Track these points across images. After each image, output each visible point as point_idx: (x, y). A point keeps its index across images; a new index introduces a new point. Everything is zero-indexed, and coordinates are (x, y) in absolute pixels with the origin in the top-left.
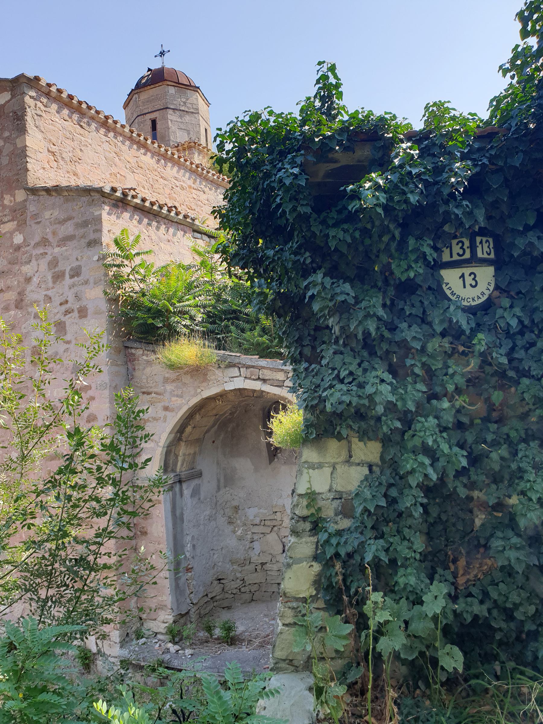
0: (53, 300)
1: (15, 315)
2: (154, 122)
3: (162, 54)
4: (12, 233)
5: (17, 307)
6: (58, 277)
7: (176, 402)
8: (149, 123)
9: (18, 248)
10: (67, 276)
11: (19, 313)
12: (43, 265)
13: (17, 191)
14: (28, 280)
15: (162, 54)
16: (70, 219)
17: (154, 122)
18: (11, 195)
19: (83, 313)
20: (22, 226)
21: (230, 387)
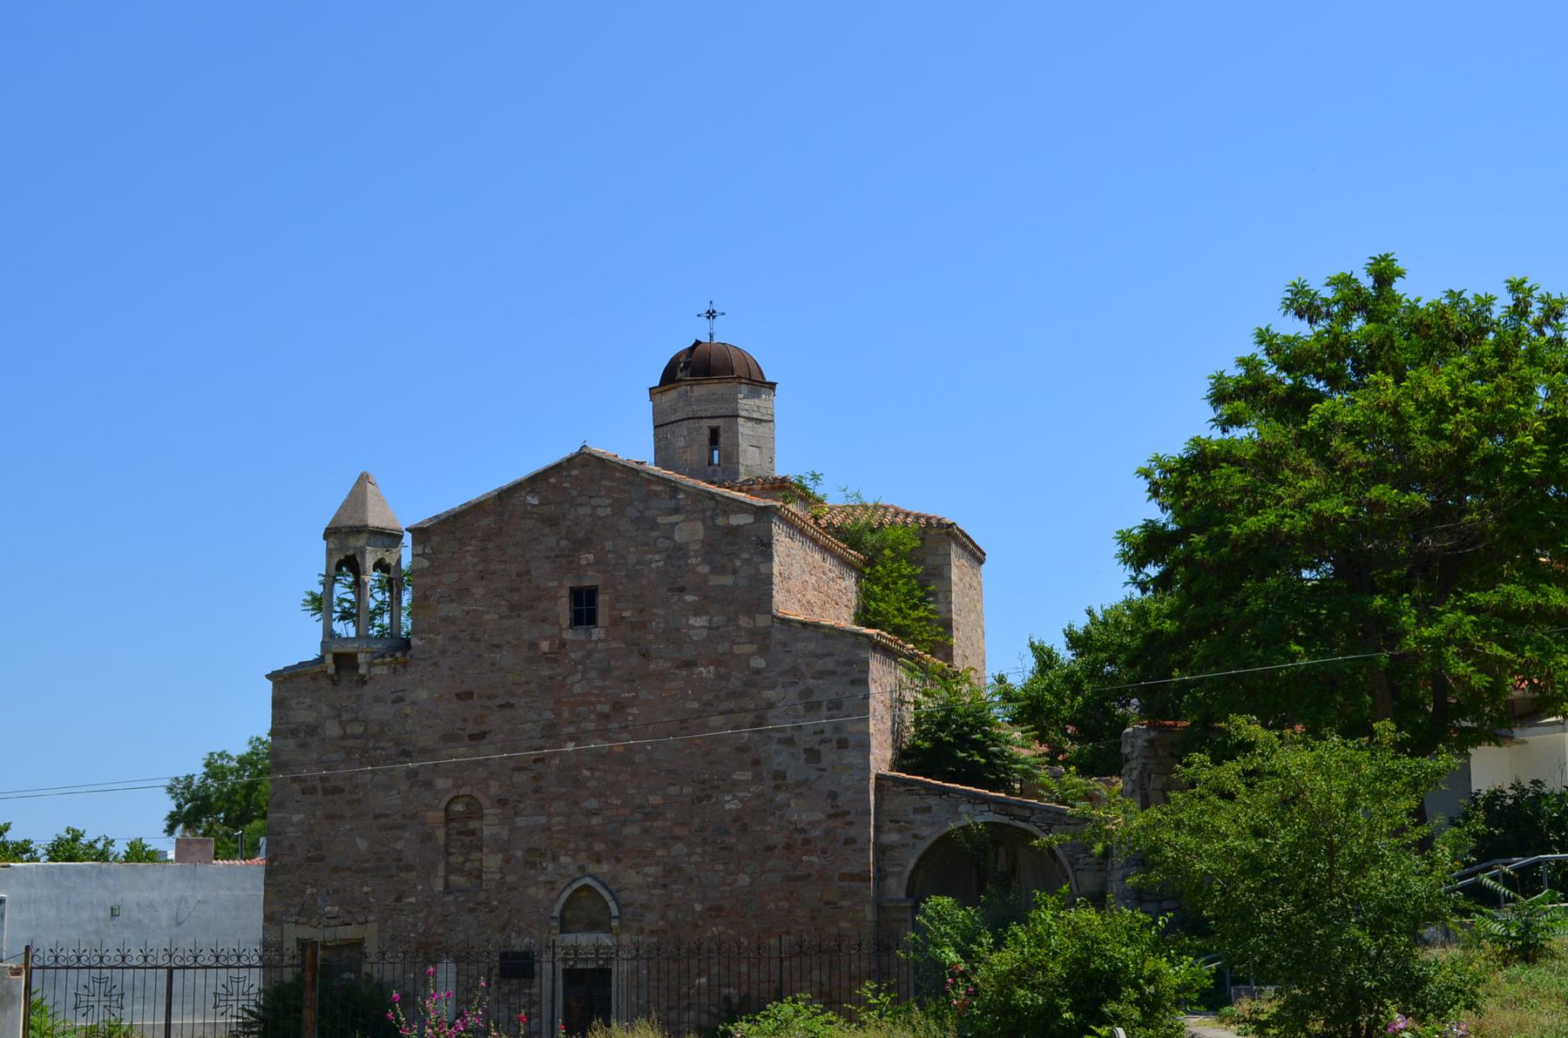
2: (714, 435)
3: (711, 314)
6: (813, 707)
8: (707, 432)
9: (758, 672)
10: (824, 708)
12: (793, 694)
15: (711, 314)
16: (829, 655)
17: (714, 435)
19: (843, 744)
20: (763, 651)
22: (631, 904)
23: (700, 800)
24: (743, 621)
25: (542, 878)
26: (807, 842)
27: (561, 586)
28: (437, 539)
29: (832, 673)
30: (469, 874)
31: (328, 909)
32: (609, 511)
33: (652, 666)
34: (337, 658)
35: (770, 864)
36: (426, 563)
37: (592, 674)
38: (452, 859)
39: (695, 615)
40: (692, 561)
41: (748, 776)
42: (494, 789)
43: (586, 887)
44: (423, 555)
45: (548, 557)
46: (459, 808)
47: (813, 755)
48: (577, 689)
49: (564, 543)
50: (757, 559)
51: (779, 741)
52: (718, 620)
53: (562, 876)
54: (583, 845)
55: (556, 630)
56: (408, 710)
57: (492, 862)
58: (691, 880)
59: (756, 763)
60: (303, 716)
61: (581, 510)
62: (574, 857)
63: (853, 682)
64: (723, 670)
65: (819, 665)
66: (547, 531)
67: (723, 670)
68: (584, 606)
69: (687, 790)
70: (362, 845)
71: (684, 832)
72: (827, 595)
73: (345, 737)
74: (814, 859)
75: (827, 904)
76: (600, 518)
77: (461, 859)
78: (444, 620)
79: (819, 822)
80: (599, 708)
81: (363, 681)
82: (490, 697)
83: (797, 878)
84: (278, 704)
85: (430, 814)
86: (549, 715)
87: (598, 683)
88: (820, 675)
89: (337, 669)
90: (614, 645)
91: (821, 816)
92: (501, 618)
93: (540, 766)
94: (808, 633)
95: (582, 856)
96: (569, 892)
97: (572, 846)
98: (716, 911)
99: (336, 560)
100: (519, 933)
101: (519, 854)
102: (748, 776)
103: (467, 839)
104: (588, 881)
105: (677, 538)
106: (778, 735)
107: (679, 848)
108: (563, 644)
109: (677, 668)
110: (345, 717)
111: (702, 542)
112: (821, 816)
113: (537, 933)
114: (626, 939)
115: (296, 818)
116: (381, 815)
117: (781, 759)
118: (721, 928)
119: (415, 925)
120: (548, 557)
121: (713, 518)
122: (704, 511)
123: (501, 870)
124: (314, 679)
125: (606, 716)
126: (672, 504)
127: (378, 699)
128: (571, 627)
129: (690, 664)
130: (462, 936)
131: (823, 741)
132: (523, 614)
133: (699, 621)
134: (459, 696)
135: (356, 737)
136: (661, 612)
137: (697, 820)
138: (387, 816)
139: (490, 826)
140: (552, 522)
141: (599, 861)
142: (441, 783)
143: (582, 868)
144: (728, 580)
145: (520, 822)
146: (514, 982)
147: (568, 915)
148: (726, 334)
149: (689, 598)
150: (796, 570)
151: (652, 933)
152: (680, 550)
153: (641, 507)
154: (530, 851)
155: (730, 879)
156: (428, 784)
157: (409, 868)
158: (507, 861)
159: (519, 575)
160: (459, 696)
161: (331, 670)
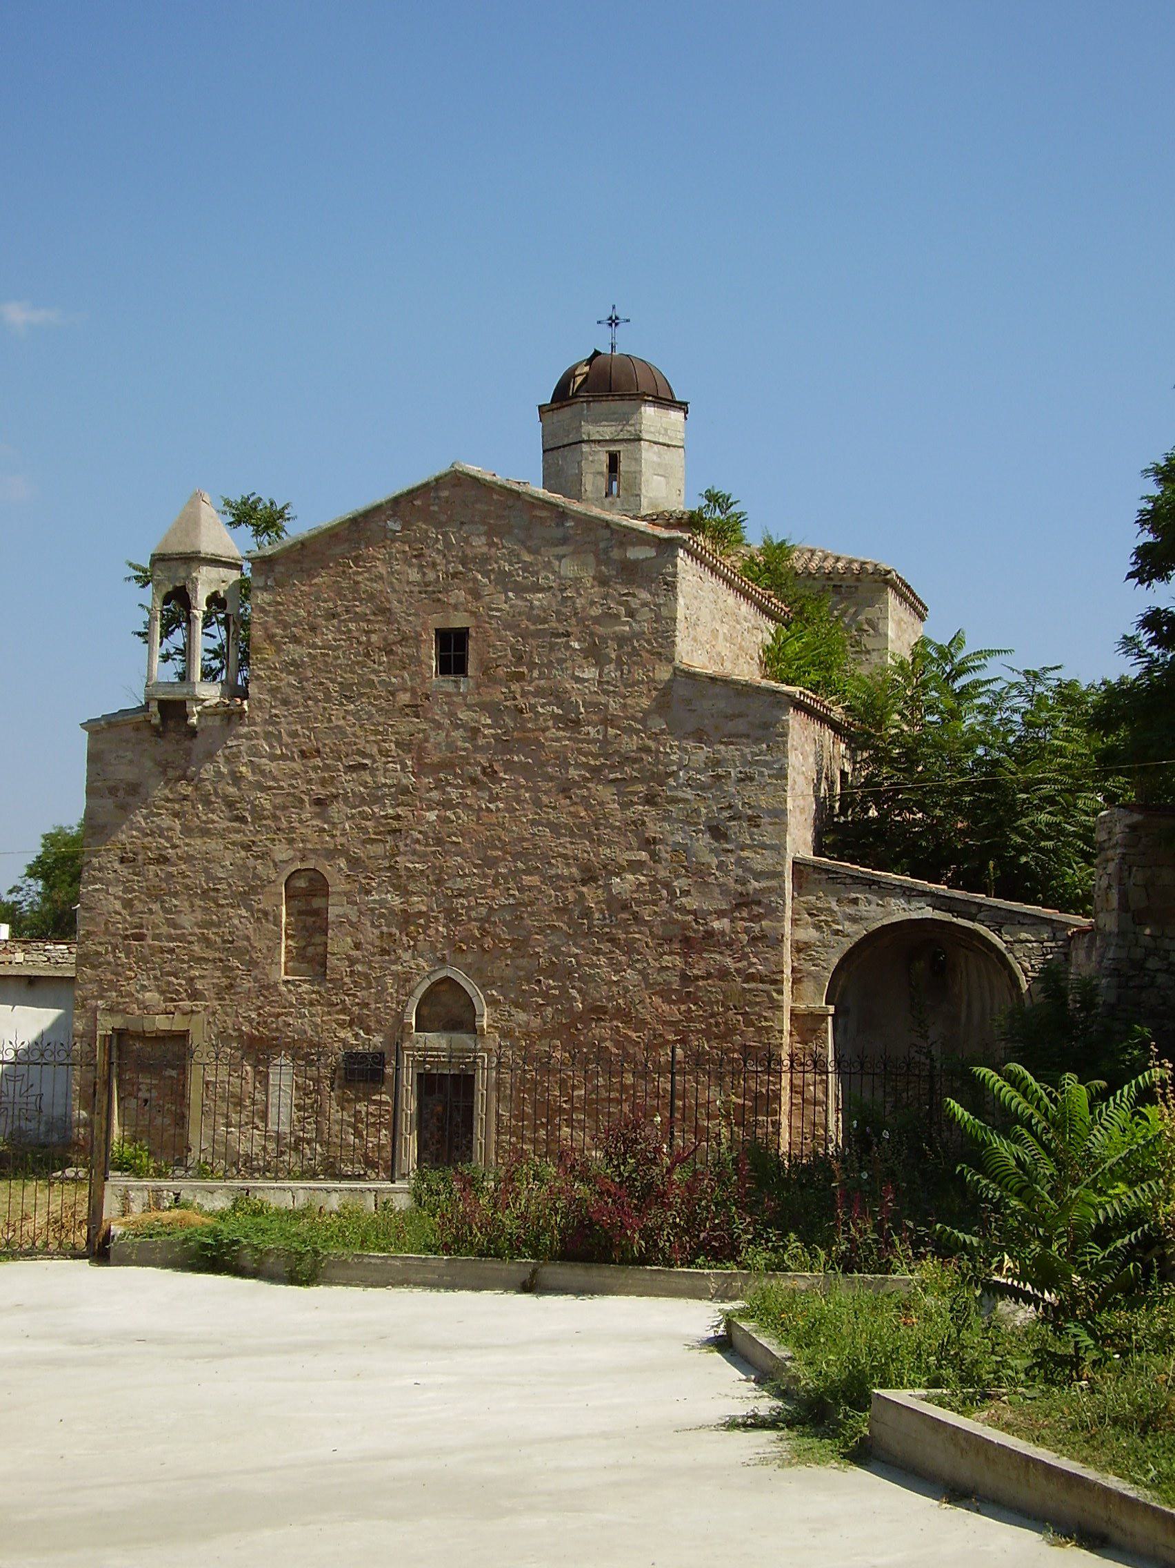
2: (614, 460)
3: (613, 321)
7: (848, 927)
8: (605, 458)
15: (613, 321)
16: (740, 716)
17: (614, 460)
21: (915, 916)
28: (282, 569)
34: (164, 705)
43: (447, 979)
47: (717, 833)
60: (124, 772)
65: (731, 726)
72: (741, 648)
74: (718, 957)
81: (193, 732)
84: (94, 758)
89: (163, 718)
94: (717, 689)
96: (426, 984)
99: (164, 591)
124: (137, 729)
125: (474, 781)
126: (558, 533)
131: (731, 818)
148: (629, 343)
150: (705, 615)
158: (357, 946)
161: (156, 720)
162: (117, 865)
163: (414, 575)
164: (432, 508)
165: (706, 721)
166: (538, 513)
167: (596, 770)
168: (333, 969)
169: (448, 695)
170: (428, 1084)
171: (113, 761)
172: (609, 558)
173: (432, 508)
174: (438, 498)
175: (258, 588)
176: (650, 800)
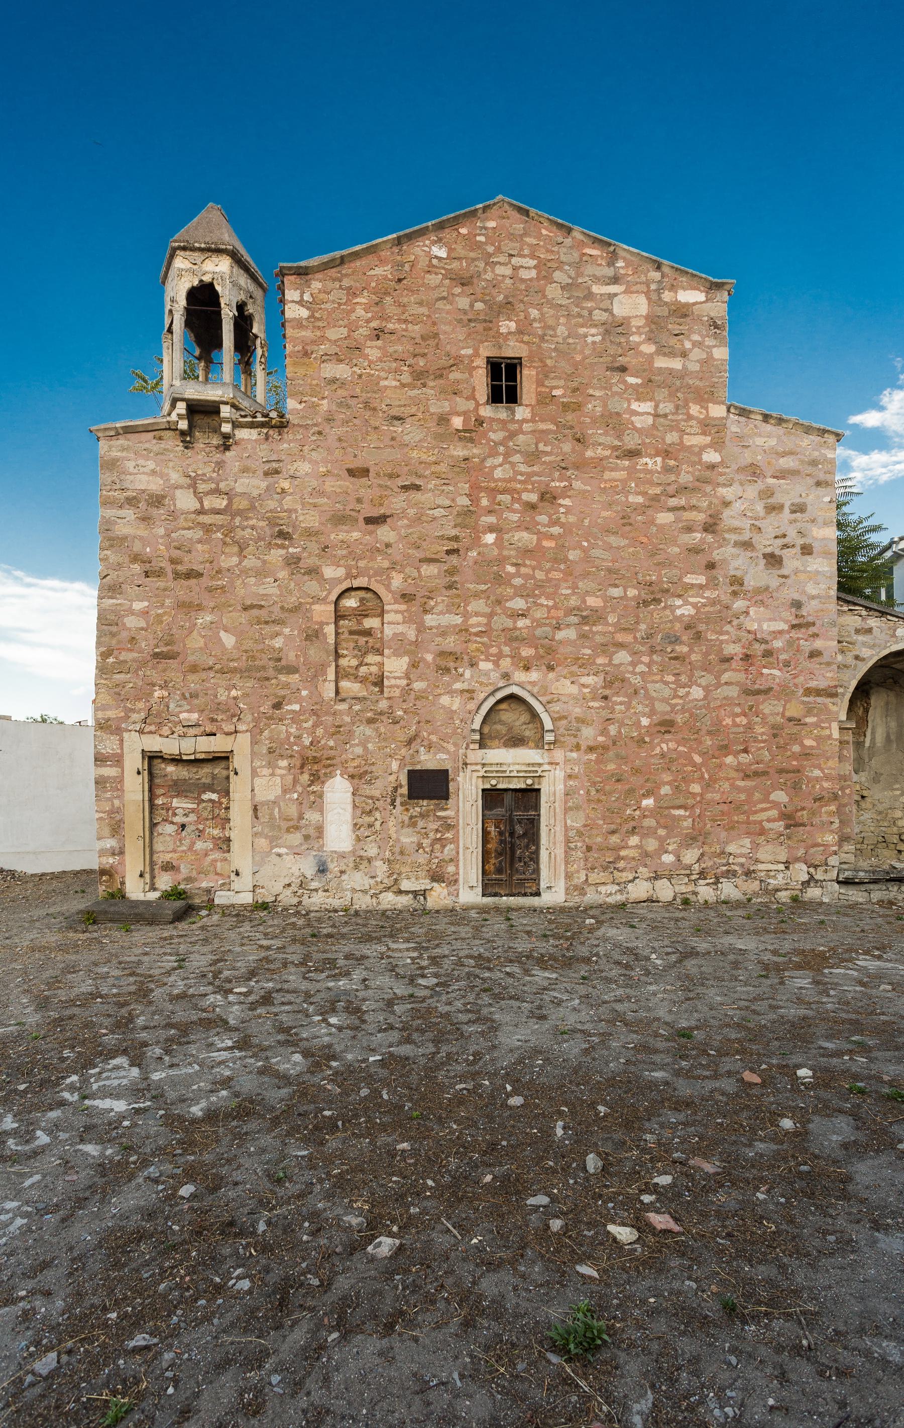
0: (763, 530)
1: (702, 540)
4: (703, 449)
5: (706, 530)
6: (773, 509)
9: (712, 467)
10: (787, 510)
11: (710, 538)
12: (751, 492)
13: (710, 405)
14: (727, 504)
16: (791, 453)
18: (702, 407)
19: (807, 550)
20: (718, 445)
22: (565, 717)
23: (646, 603)
24: (694, 410)
25: (458, 686)
26: (768, 654)
27: (476, 354)
29: (794, 473)
30: (363, 680)
31: (183, 716)
32: (533, 273)
33: (589, 453)
35: (725, 677)
36: (305, 313)
37: (517, 458)
38: (343, 662)
39: (638, 400)
40: (635, 338)
41: (702, 580)
42: (397, 581)
44: (301, 303)
45: (460, 321)
46: (351, 602)
47: (773, 560)
48: (498, 473)
49: (479, 306)
50: (709, 342)
51: (736, 544)
52: (666, 407)
53: (481, 684)
54: (506, 650)
55: (471, 405)
56: (286, 485)
57: (395, 666)
58: (636, 692)
59: (711, 566)
61: (500, 270)
62: (496, 664)
63: (818, 484)
64: (672, 463)
66: (458, 290)
67: (672, 463)
68: (504, 381)
69: (632, 592)
70: (229, 640)
71: (628, 638)
73: (201, 512)
74: (776, 672)
75: (790, 720)
76: (523, 281)
77: (354, 662)
78: (334, 381)
79: (781, 632)
80: (525, 496)
82: (391, 476)
83: (758, 692)
85: (316, 607)
86: (464, 501)
87: (523, 468)
88: (781, 475)
89: (191, 426)
90: (542, 426)
91: (784, 627)
92: (403, 385)
93: (454, 560)
95: (506, 663)
96: (491, 701)
97: (494, 650)
98: (666, 726)
100: (429, 747)
101: (429, 657)
102: (702, 580)
103: (362, 640)
104: (515, 690)
105: (616, 311)
106: (733, 537)
107: (622, 657)
108: (480, 422)
109: (617, 457)
110: (202, 487)
111: (647, 317)
112: (784, 627)
113: (451, 748)
114: (559, 755)
115: (138, 606)
116: (252, 607)
117: (737, 562)
118: (672, 745)
119: (299, 737)
120: (460, 321)
121: (658, 291)
122: (647, 284)
123: (407, 676)
125: (533, 507)
126: (610, 272)
127: (245, 470)
128: (487, 403)
129: (633, 454)
130: (359, 750)
131: (786, 546)
132: (431, 384)
133: (646, 407)
134: (351, 472)
135: (218, 512)
136: (597, 393)
137: (643, 627)
138: (261, 607)
139: (393, 623)
140: (465, 282)
141: (527, 668)
142: (329, 572)
143: (506, 676)
144: (676, 364)
145: (430, 620)
146: (425, 802)
147: (486, 730)
149: (631, 380)
151: (591, 749)
152: (617, 328)
153: (573, 274)
154: (442, 654)
155: (682, 692)
156: (313, 572)
157: (291, 670)
158: (414, 665)
159: (422, 337)
160: (351, 472)
162: (142, 580)
163: (463, 303)
164: (478, 238)
165: (759, 457)
166: (588, 251)
167: (656, 498)
168: (391, 687)
169: (503, 422)
170: (492, 797)
171: (131, 470)
172: (660, 299)
173: (478, 238)
174: (486, 228)
175: (293, 301)
176: (709, 528)
